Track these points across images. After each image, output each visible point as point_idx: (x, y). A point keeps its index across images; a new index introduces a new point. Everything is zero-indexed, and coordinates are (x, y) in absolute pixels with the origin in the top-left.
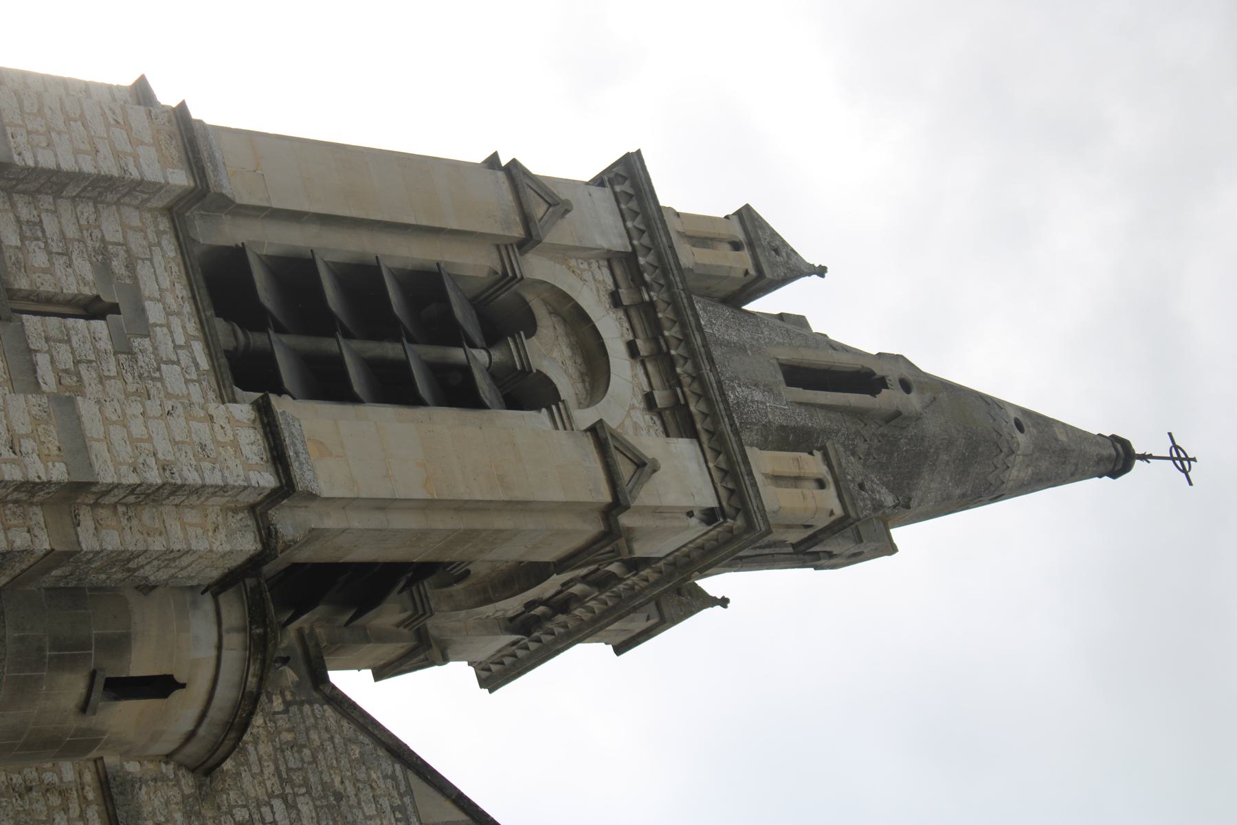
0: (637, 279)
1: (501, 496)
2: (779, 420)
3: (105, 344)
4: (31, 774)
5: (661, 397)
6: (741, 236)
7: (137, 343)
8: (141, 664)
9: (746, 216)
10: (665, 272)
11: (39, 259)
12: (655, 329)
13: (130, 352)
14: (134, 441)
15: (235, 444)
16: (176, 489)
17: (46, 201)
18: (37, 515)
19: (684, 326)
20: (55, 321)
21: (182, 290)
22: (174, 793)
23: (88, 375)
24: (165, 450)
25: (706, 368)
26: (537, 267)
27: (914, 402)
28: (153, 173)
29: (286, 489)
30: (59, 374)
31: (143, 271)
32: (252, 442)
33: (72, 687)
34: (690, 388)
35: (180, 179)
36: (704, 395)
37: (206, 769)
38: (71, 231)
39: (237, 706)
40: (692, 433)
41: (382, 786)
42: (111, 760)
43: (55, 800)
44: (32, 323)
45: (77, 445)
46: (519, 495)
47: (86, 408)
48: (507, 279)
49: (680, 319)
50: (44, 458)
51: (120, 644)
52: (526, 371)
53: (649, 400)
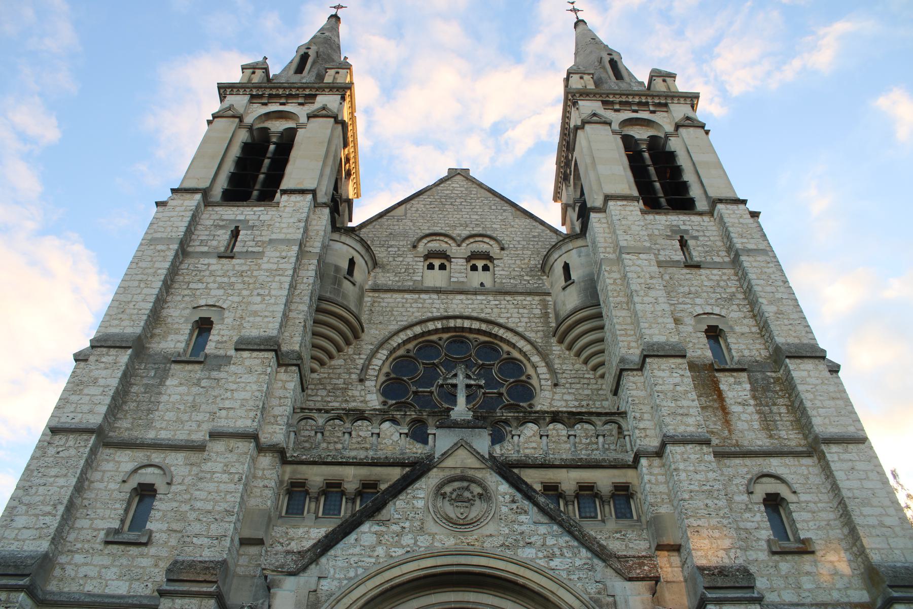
0: (261, 96)
1: (326, 144)
4: (366, 309)
5: (301, 100)
7: (251, 223)
8: (345, 265)
9: (244, 68)
10: (261, 88)
11: (214, 243)
12: (278, 96)
14: (288, 227)
15: (295, 202)
16: (307, 221)
17: (193, 237)
18: (305, 261)
19: (280, 88)
20: (237, 243)
21: (235, 209)
22: (380, 274)
23: (259, 239)
26: (249, 120)
27: (314, 48)
28: (195, 203)
29: (314, 192)
30: (257, 246)
31: (225, 217)
32: (294, 198)
33: (347, 284)
34: (300, 92)
35: (198, 196)
36: (304, 88)
37: (375, 264)
38: (207, 233)
39: (363, 245)
40: (316, 95)
41: (390, 222)
42: (367, 287)
43: (376, 304)
45: (287, 242)
46: (327, 140)
48: (250, 128)
49: (277, 88)
51: (337, 269)
52: (282, 133)
53: (300, 104)
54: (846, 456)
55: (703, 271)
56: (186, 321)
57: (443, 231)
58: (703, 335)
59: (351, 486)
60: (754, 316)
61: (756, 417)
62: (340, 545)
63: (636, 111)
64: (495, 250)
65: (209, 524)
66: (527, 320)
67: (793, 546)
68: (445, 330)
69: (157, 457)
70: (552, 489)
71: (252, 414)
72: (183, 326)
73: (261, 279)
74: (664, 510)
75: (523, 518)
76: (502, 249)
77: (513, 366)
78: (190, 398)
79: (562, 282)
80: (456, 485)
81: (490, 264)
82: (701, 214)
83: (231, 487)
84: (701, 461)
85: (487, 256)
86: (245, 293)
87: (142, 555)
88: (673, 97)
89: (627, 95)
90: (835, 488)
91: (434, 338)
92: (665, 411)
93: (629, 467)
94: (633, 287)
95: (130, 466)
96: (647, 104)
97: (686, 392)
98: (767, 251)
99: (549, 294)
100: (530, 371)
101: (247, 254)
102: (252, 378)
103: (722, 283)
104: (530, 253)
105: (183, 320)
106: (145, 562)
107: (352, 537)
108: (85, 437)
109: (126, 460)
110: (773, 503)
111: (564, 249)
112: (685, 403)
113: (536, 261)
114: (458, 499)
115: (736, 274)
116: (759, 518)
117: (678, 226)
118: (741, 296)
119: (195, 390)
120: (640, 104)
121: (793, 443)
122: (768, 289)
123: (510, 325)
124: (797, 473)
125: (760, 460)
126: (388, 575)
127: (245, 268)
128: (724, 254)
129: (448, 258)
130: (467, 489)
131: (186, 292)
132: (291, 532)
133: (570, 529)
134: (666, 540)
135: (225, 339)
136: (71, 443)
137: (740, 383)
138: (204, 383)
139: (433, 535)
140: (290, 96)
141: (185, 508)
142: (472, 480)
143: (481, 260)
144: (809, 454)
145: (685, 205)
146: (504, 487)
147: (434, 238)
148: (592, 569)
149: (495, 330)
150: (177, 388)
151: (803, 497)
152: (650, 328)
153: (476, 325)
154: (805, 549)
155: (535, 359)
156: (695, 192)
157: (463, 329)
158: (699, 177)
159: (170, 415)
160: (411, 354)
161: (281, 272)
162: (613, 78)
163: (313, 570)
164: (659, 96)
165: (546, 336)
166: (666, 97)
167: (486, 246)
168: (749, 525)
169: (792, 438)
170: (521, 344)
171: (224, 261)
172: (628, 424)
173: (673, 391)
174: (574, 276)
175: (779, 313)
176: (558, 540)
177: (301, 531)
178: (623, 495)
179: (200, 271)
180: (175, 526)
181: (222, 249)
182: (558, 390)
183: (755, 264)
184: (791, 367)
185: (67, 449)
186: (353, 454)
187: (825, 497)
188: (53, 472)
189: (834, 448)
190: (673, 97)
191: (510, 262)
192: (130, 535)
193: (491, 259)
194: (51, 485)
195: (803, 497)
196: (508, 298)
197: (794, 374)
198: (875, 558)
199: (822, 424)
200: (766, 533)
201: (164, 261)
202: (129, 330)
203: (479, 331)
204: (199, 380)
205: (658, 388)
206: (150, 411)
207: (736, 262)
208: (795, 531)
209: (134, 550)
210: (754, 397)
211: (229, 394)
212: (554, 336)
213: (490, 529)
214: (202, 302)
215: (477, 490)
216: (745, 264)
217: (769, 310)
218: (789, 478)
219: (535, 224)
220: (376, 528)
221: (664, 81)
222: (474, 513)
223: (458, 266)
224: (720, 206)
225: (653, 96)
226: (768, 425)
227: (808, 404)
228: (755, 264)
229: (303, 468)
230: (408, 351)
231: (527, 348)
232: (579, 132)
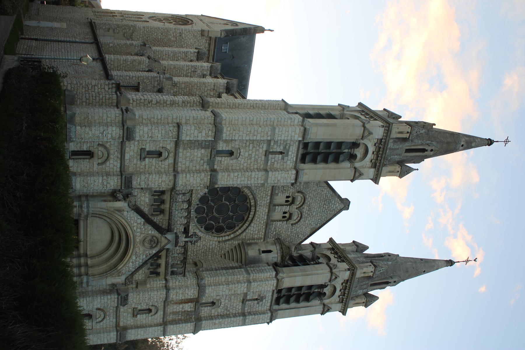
0: (380, 143)
2: (398, 160)
3: (280, 158)
6: (409, 131)
11: (275, 147)
13: (284, 159)
23: (276, 163)
24: (279, 178)
25: (382, 160)
26: (362, 141)
30: (271, 162)
31: (291, 147)
32: (293, 177)
36: (380, 163)
40: (375, 167)
44: (270, 156)
47: (270, 173)
49: (383, 151)
50: (261, 180)
53: (371, 161)
54: (159, 331)
55: (241, 304)
56: (233, 147)
57: (306, 202)
58: (212, 300)
59: (162, 207)
60: (218, 315)
61: (178, 310)
62: (137, 215)
63: (340, 290)
64: (292, 222)
65: (144, 181)
66: (252, 232)
67: (135, 313)
68: (250, 205)
69: (172, 155)
70: (160, 257)
71: (184, 184)
72: (230, 146)
73: (247, 174)
74: (148, 286)
75: (144, 256)
76: (292, 224)
77: (231, 227)
78: (195, 158)
79: (262, 250)
80: (156, 240)
81: (286, 219)
82: (271, 306)
83: (157, 184)
84: (160, 298)
85: (290, 218)
86: (245, 165)
87: (137, 160)
88: (345, 306)
89: (349, 290)
90: (151, 326)
91: (248, 201)
92: (178, 291)
93: (165, 276)
94: (230, 286)
95: (168, 147)
96: (344, 296)
97: (185, 296)
98: (244, 324)
99: (264, 240)
100: (228, 233)
101: (267, 161)
102: (198, 181)
103: (234, 308)
104: (289, 234)
105: (233, 146)
106: (135, 161)
107: (140, 217)
108: (176, 137)
109: (170, 146)
110: (150, 311)
111: (279, 251)
112: (181, 296)
113: (283, 236)
114: (151, 241)
115: (238, 313)
116: (145, 307)
117: (265, 298)
118: (228, 313)
119: (199, 159)
120: (345, 293)
121: (168, 318)
122: (226, 323)
123: (249, 228)
124: (158, 317)
125: (162, 309)
126: (128, 227)
127: (259, 161)
128: (249, 311)
129: (290, 205)
130: (155, 243)
131: (248, 144)
132: (147, 193)
133: (145, 263)
134: (139, 285)
135: (223, 163)
136: (174, 133)
137: (191, 308)
138: (202, 162)
139: (140, 236)
140: (378, 157)
141: (153, 167)
142: (157, 244)
143: (287, 217)
144: (163, 321)
145: (277, 302)
146: (154, 252)
147: (303, 199)
148: (129, 271)
149: (248, 223)
150: (200, 153)
151: (150, 318)
152: (212, 289)
153: (251, 216)
154: (134, 315)
155: (232, 236)
156: (284, 306)
157: (250, 211)
158: (291, 309)
159: (188, 154)
160: (241, 193)
161: (249, 179)
162: (373, 283)
163: (129, 209)
164: (346, 301)
165: (243, 239)
166: (345, 303)
167: (295, 218)
168: (142, 305)
169: (170, 318)
170: (240, 231)
171: (264, 153)
172: (180, 278)
173: (185, 293)
174: (264, 255)
175: (215, 324)
176: (140, 261)
177: (147, 196)
178: (158, 274)
179: (259, 146)
180: (147, 166)
181: (271, 151)
182: (217, 243)
183: (238, 321)
184: (192, 324)
185: (172, 133)
186: (174, 206)
187: (150, 322)
188: (163, 132)
189: (162, 329)
190: (345, 306)
191: (284, 227)
192: (145, 154)
193: (287, 220)
194: (159, 133)
195: (150, 318)
196: (264, 227)
197: (189, 324)
198: (129, 331)
199: (170, 328)
200: (139, 308)
201: (261, 137)
202: (224, 135)
203: (248, 217)
204: (203, 160)
205: (187, 290)
206: (190, 147)
207: (244, 315)
208: (140, 314)
209: (139, 157)
210: (185, 311)
211: (192, 175)
212: (242, 242)
213: (141, 249)
214: (242, 151)
215: (154, 245)
216: (238, 318)
217: (217, 321)
218: (156, 315)
219: (306, 236)
220: (142, 223)
221: (364, 303)
222: (146, 245)
223: (286, 209)
224: (270, 314)
225: (347, 299)
226: (174, 313)
227: (178, 325)
228: (238, 321)
229: (169, 193)
230: (243, 192)
231: (238, 233)
232: (329, 270)
